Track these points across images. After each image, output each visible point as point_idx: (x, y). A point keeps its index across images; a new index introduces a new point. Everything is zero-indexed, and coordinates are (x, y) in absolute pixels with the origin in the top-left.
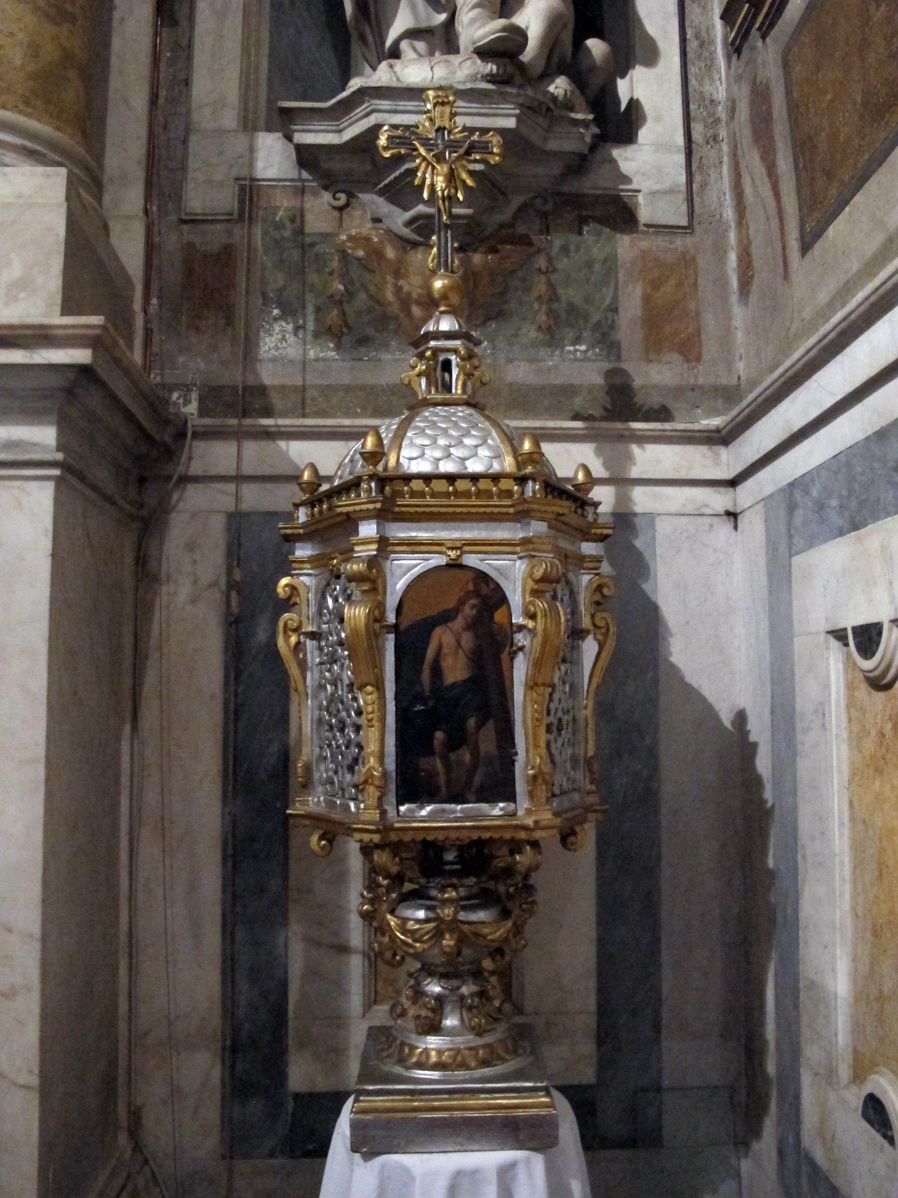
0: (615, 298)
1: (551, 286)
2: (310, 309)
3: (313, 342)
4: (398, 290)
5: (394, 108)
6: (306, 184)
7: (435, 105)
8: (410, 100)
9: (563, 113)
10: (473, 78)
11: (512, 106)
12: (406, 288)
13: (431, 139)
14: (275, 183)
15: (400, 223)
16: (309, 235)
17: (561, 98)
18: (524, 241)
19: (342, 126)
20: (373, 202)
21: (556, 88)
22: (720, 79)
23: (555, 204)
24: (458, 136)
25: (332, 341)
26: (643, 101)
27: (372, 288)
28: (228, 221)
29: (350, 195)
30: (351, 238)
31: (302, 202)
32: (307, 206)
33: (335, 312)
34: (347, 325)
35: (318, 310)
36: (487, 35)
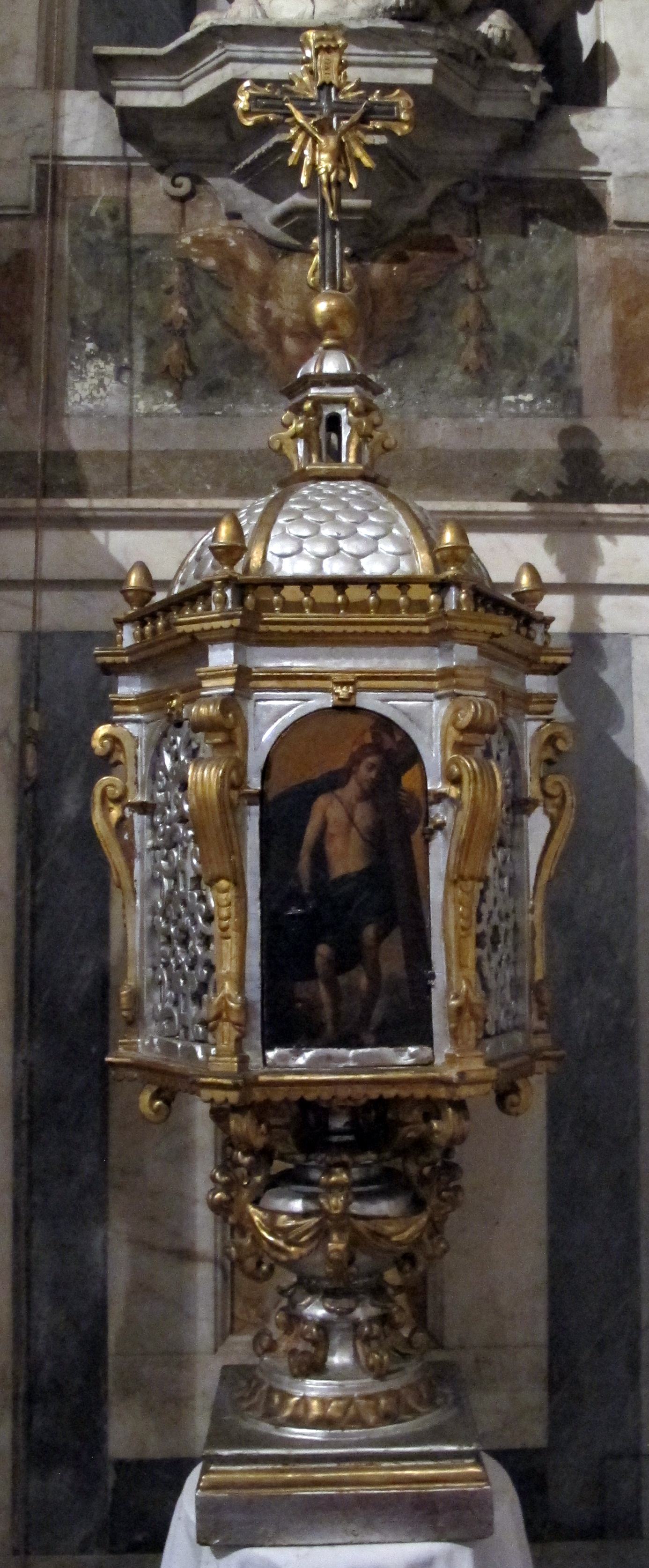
0: (575, 327)
1: (482, 308)
2: (139, 342)
3: (144, 390)
4: (265, 314)
5: (258, 55)
6: (133, 164)
7: (317, 51)
8: (281, 44)
9: (501, 62)
11: (428, 53)
12: (276, 313)
13: (311, 100)
14: (88, 163)
15: (267, 220)
16: (137, 236)
17: (497, 41)
18: (445, 245)
19: (184, 82)
20: (229, 190)
21: (490, 27)
23: (489, 192)
24: (350, 95)
25: (170, 387)
26: (614, 46)
27: (227, 312)
28: (22, 217)
29: (197, 180)
30: (197, 241)
31: (128, 189)
32: (135, 195)
33: (175, 347)
35: (150, 343)
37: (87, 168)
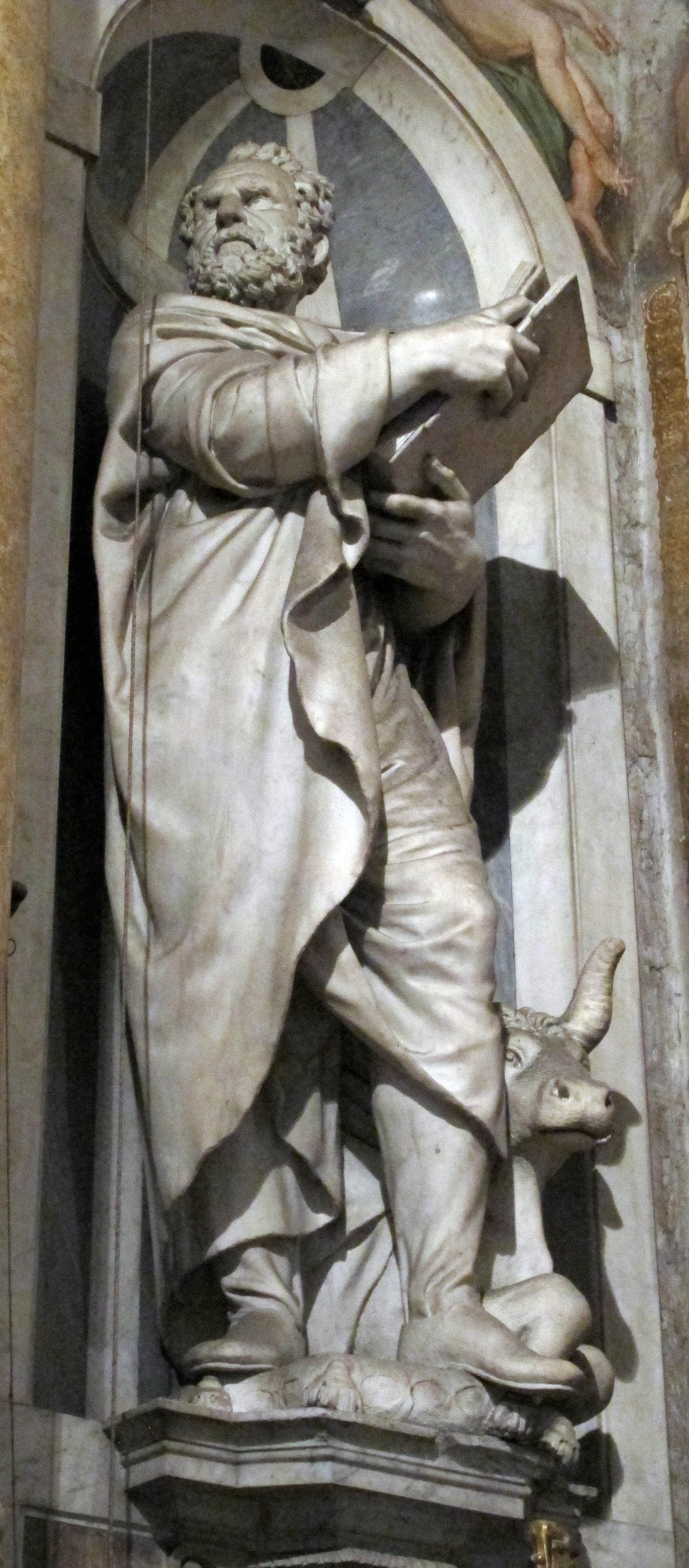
6: (134, 1532)
8: (384, 1448)
10: (475, 1426)
11: (522, 1481)
14: (82, 1523)
21: (562, 1441)
36: (535, 1379)
37: (83, 1530)
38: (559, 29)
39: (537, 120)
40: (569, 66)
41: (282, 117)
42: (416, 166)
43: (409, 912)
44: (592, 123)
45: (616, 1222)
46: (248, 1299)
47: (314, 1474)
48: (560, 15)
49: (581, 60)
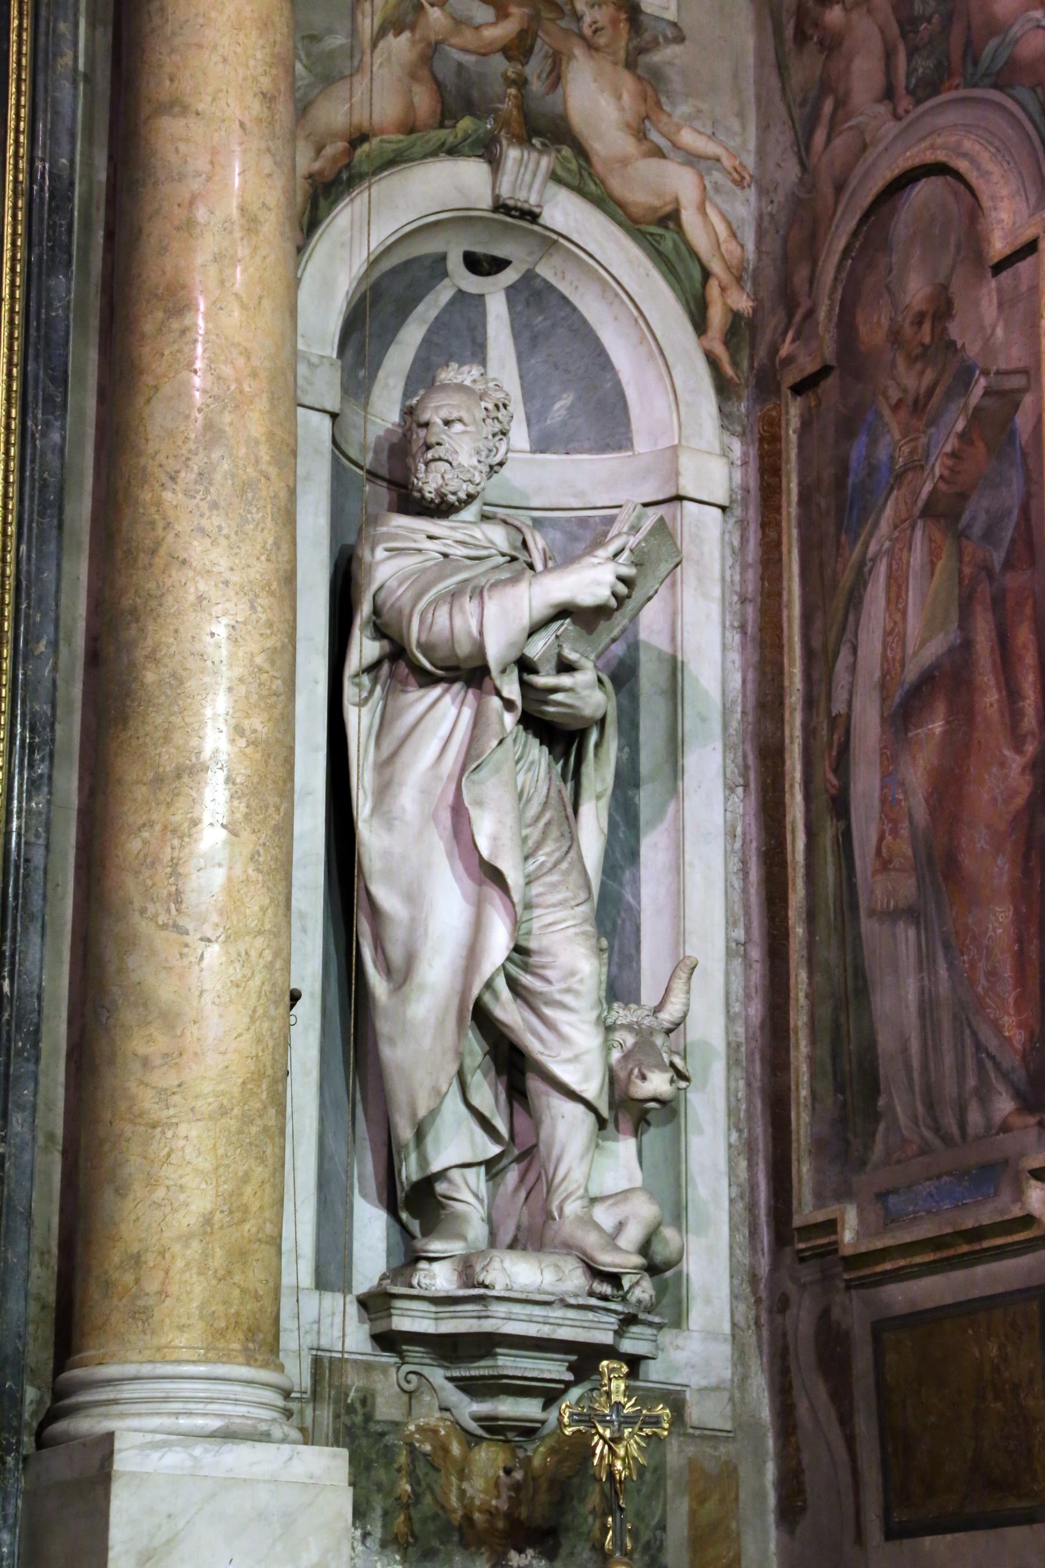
3: (381, 1553)
4: (462, 1493)
12: (470, 1492)
13: (607, 1415)
16: (379, 1422)
22: (763, 1250)
25: (398, 1552)
27: (438, 1490)
30: (420, 1429)
33: (402, 1517)
34: (413, 1534)
35: (386, 1514)
38: (701, 177)
39: (680, 268)
40: (710, 210)
41: (482, 296)
42: (584, 322)
43: (543, 967)
44: (726, 256)
45: (701, 1131)
46: (451, 1202)
47: (480, 1326)
48: (703, 165)
49: (718, 199)
